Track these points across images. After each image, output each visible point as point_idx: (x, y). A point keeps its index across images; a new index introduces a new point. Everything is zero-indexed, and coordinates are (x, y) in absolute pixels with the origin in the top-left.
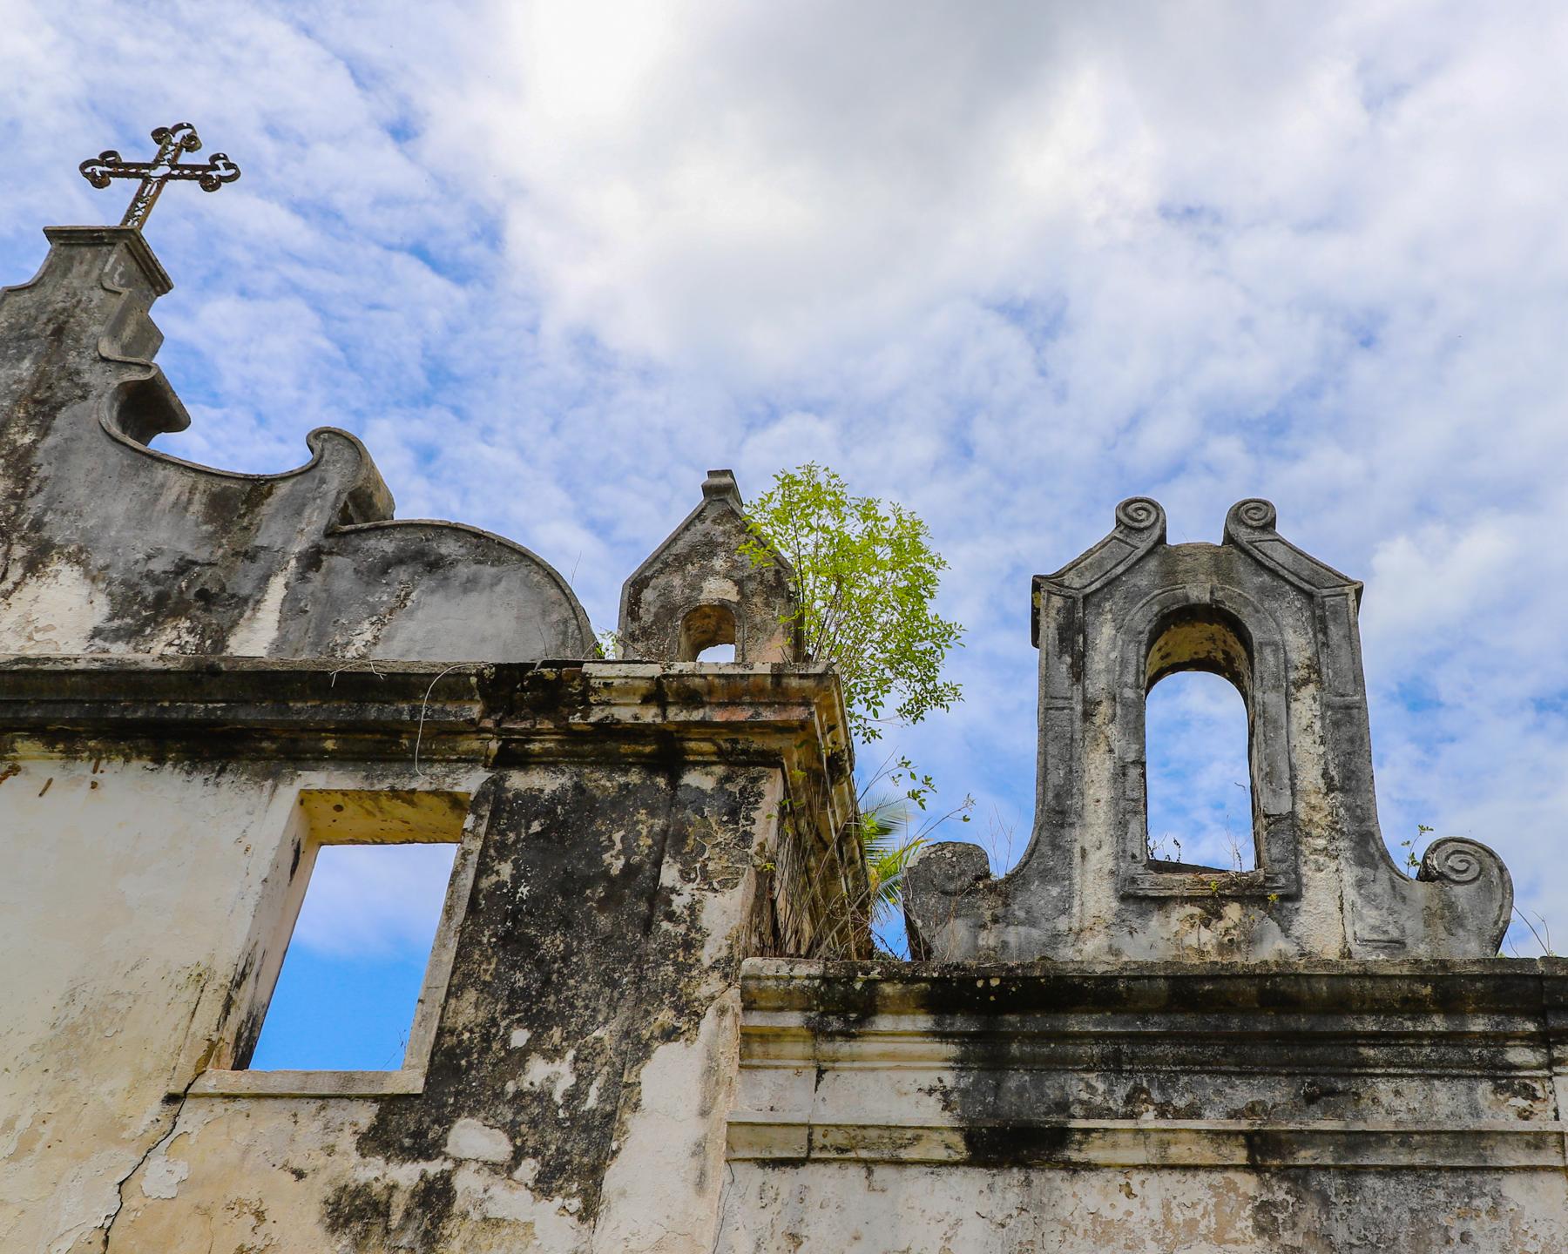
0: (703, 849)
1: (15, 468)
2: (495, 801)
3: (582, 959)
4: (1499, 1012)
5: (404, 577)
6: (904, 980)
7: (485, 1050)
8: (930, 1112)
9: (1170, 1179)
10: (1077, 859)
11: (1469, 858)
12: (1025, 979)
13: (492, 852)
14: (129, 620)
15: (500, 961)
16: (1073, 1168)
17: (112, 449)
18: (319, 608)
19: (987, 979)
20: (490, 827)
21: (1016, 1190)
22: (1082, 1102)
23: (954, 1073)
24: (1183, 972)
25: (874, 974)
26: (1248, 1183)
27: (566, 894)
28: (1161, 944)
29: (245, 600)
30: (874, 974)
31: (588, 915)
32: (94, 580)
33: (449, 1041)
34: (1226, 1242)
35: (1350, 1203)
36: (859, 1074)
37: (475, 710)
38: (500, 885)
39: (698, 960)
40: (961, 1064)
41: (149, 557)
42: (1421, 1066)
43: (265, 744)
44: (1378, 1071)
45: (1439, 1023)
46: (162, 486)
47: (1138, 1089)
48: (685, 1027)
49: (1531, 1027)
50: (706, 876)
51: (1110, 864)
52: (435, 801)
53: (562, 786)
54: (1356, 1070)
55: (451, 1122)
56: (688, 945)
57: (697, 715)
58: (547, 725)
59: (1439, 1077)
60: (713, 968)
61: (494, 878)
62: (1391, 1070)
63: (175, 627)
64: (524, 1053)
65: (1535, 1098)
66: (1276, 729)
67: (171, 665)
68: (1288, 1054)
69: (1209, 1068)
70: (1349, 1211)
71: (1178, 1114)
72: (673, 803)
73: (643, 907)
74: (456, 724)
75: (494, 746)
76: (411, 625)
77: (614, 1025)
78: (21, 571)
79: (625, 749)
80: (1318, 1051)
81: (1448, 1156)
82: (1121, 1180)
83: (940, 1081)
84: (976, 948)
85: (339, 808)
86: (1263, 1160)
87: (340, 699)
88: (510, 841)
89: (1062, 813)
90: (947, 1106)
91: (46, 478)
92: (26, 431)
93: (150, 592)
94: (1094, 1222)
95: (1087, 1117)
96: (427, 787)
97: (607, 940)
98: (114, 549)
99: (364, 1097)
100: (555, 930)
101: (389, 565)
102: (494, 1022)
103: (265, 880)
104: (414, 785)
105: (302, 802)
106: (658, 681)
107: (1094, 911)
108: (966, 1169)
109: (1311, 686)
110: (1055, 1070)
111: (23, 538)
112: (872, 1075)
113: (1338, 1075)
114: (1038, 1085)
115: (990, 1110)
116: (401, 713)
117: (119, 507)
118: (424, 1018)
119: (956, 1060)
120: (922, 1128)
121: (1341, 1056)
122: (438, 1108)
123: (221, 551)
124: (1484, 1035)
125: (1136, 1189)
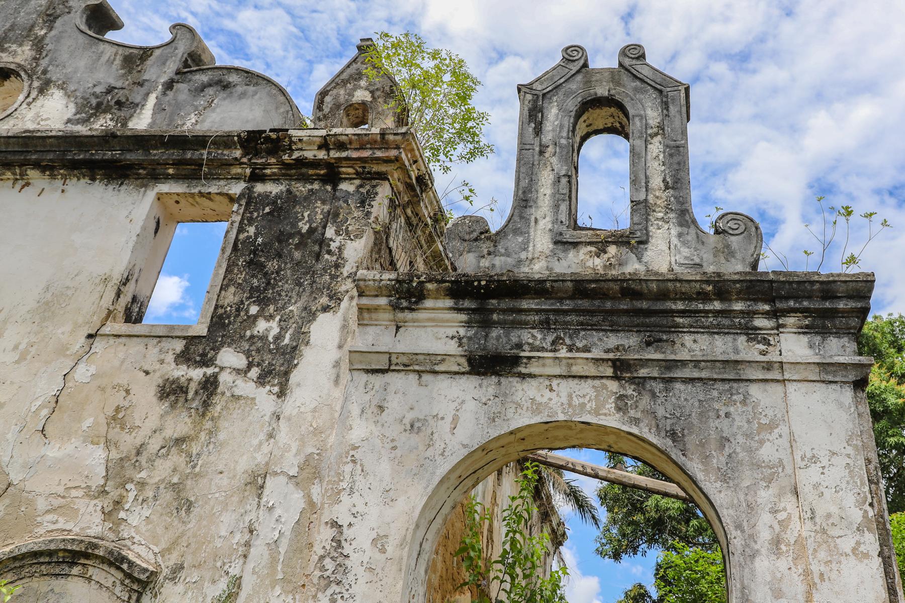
0: (347, 220)
1: (36, 45)
3: (285, 273)
5: (211, 92)
6: (437, 281)
8: (452, 347)
9: (572, 383)
12: (498, 281)
13: (246, 222)
14: (84, 115)
15: (247, 273)
16: (523, 376)
17: (81, 37)
18: (171, 108)
19: (479, 281)
21: (493, 387)
22: (529, 344)
23: (465, 329)
24: (580, 278)
25: (422, 279)
26: (613, 386)
29: (137, 105)
32: (69, 96)
34: (600, 415)
35: (666, 396)
36: (418, 329)
38: (249, 237)
39: (341, 273)
40: (468, 324)
41: (95, 86)
43: (141, 171)
44: (685, 330)
45: (717, 305)
46: (102, 52)
47: (558, 338)
48: (333, 306)
50: (347, 233)
52: (221, 198)
53: (281, 190)
54: (673, 329)
55: (219, 349)
56: (337, 266)
60: (348, 277)
61: (246, 234)
63: (104, 118)
65: (769, 345)
67: (94, 133)
68: (637, 320)
69: (595, 327)
70: (666, 400)
71: (578, 350)
72: (335, 198)
73: (317, 248)
74: (229, 160)
75: (248, 171)
76: (214, 115)
77: (299, 304)
78: (36, 93)
80: (652, 319)
81: (720, 373)
82: (547, 383)
83: (458, 333)
84: (479, 267)
85: (177, 202)
86: (621, 374)
87: (174, 149)
88: (254, 217)
90: (460, 345)
91: (50, 50)
92: (42, 29)
93: (94, 102)
94: (532, 404)
95: (530, 351)
96: (216, 191)
97: (298, 264)
98: (79, 82)
99: (179, 337)
100: (273, 258)
101: (205, 87)
103: (138, 235)
104: (210, 190)
105: (159, 199)
108: (468, 376)
110: (516, 328)
111: (38, 78)
112: (423, 329)
113: (664, 332)
114: (507, 335)
115: (482, 347)
116: (202, 155)
117: (82, 63)
118: (209, 300)
119: (465, 322)
120: (445, 355)
122: (213, 343)
123: (127, 82)
125: (555, 387)
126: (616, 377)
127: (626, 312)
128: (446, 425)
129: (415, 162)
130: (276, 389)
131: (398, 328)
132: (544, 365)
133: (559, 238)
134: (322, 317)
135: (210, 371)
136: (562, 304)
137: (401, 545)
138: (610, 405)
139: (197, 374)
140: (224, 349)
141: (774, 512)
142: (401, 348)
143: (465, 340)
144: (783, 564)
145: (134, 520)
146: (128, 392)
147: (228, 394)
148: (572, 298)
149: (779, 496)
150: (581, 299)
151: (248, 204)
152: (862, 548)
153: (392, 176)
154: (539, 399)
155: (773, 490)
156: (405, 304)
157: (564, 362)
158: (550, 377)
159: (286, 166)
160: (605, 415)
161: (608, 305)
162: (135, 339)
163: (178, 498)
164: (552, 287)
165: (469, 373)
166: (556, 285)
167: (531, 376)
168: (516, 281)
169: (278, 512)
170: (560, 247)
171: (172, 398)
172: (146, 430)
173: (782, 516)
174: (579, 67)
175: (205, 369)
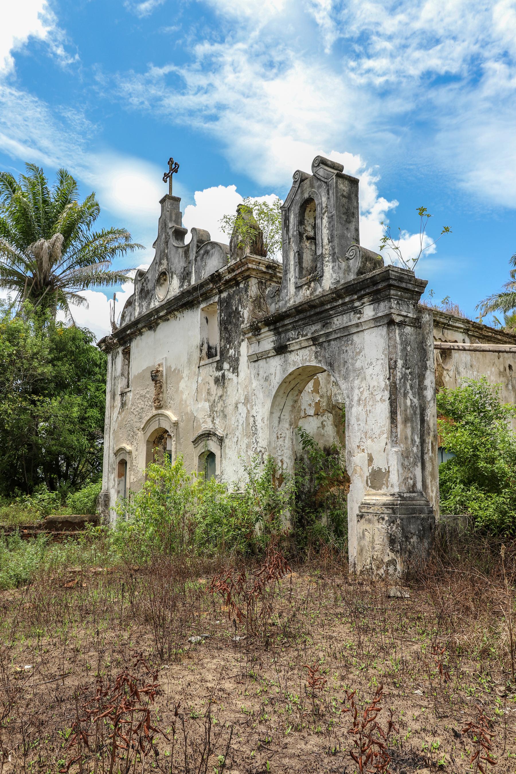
2: (220, 301)
37: (211, 286)
40: (275, 335)
47: (299, 332)
57: (235, 274)
68: (318, 317)
72: (239, 292)
126: (314, 345)
129: (260, 263)
139: (220, 373)
142: (261, 350)
144: (360, 408)
149: (361, 381)
152: (383, 398)
154: (295, 360)
155: (359, 380)
158: (297, 350)
167: (293, 351)
172: (214, 395)
173: (361, 390)
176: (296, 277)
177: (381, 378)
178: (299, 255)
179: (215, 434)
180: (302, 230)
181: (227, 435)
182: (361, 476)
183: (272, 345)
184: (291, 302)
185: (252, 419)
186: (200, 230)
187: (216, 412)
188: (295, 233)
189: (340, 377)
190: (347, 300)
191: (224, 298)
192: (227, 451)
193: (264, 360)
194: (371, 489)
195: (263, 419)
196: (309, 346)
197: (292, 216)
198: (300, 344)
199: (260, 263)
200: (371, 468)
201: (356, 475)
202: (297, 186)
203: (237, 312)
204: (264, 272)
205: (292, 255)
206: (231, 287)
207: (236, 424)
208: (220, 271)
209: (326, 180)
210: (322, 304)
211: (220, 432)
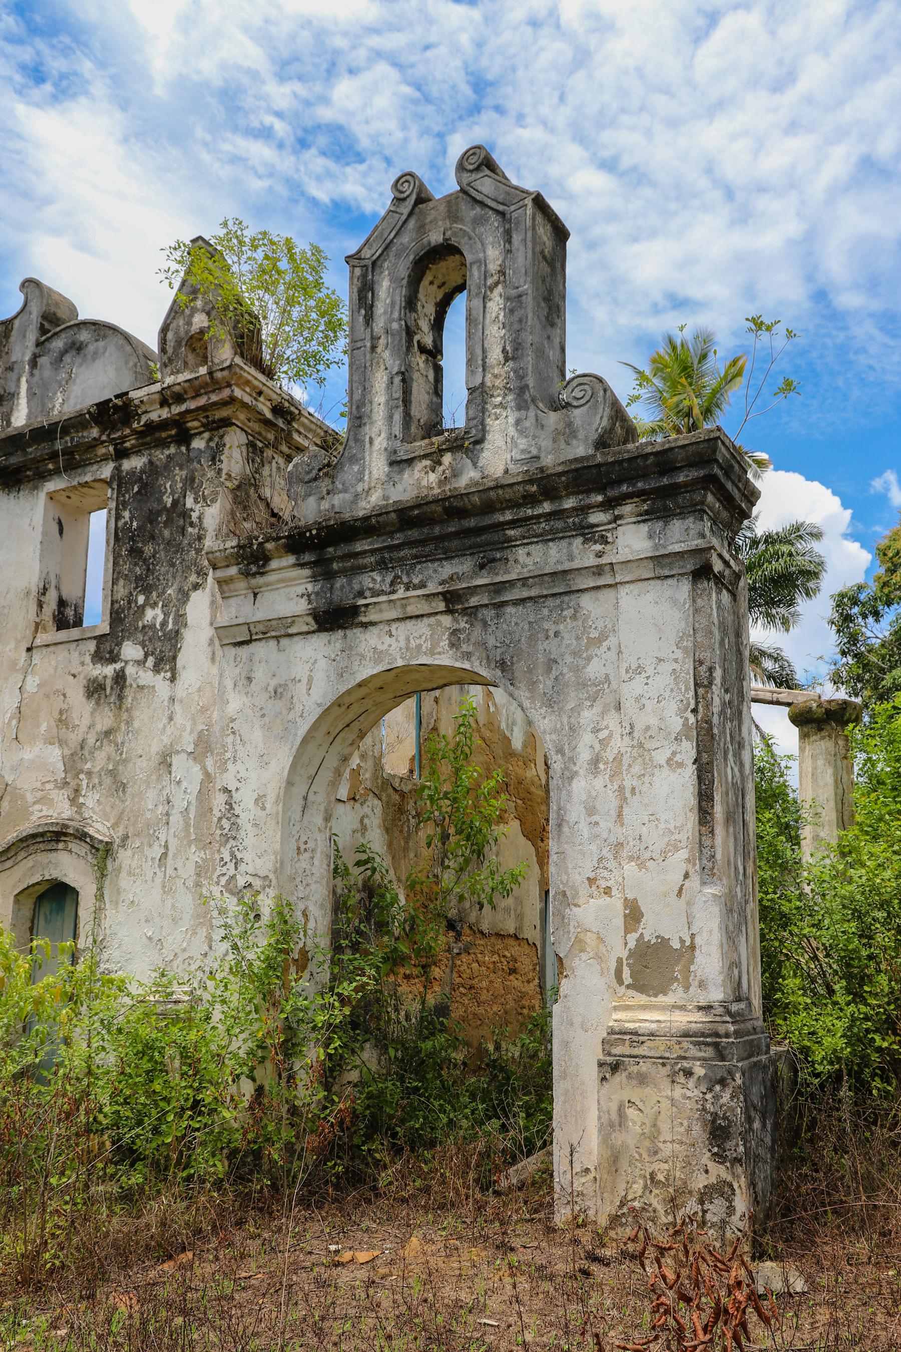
2: (119, 480)
4: (582, 492)
7: (130, 608)
10: (367, 446)
11: (586, 387)
12: (327, 527)
19: (310, 531)
20: (118, 494)
22: (370, 589)
25: (260, 540)
27: (151, 523)
28: (409, 488)
30: (260, 540)
31: (160, 531)
33: (116, 606)
40: (314, 578)
42: (541, 535)
47: (397, 577)
49: (600, 498)
50: (205, 500)
51: (385, 445)
56: (200, 538)
57: (183, 408)
58: (127, 431)
59: (552, 540)
62: (525, 541)
64: (143, 607)
65: (607, 543)
66: (476, 325)
68: (468, 542)
69: (429, 558)
71: (416, 587)
72: (190, 460)
79: (164, 435)
81: (550, 588)
84: (320, 511)
89: (360, 418)
102: (131, 593)
106: (161, 392)
107: (376, 476)
109: (500, 286)
113: (497, 549)
114: (350, 583)
119: (312, 577)
121: (496, 538)
124: (574, 509)
126: (449, 611)
127: (456, 534)
128: (302, 687)
129: (260, 393)
130: (169, 675)
131: (255, 595)
132: (381, 611)
133: (393, 458)
134: (195, 596)
135: (118, 666)
136: (392, 538)
137: (277, 802)
138: (445, 643)
139: (109, 670)
140: (125, 643)
141: (596, 731)
142: (260, 616)
143: (313, 597)
144: (599, 782)
145: (90, 803)
146: (64, 695)
147: (135, 686)
148: (401, 530)
149: (603, 714)
150: (411, 529)
151: (119, 486)
152: (678, 758)
153: (237, 419)
155: (597, 709)
156: (254, 569)
157: (398, 603)
159: (140, 434)
160: (440, 653)
161: (437, 530)
162: (60, 646)
163: (115, 782)
164: (378, 522)
165: (319, 630)
166: (381, 519)
167: (373, 624)
168: (343, 523)
169: (184, 784)
170: (396, 468)
171: (96, 696)
172: (83, 728)
173: (603, 735)
174: (410, 207)
175: (114, 665)
176: (391, 437)
177: (671, 708)
178: (404, 381)
179: (82, 836)
180: (411, 323)
181: (125, 838)
182: (599, 958)
183: (301, 606)
184: (375, 498)
185: (220, 800)
186: (50, 289)
187: (89, 774)
188: (395, 326)
189: (532, 699)
190: (569, 503)
191: (132, 472)
192: (124, 881)
193: (272, 643)
194: (631, 992)
195: (260, 801)
196: (429, 615)
197: (386, 283)
198: (404, 606)
199: (260, 393)
200: (632, 939)
201: (584, 956)
202: (405, 209)
203: (179, 512)
204: (266, 422)
205: (380, 381)
206: (162, 444)
207: (161, 809)
208: (132, 395)
209: (501, 208)
210: (489, 507)
211: (99, 830)
